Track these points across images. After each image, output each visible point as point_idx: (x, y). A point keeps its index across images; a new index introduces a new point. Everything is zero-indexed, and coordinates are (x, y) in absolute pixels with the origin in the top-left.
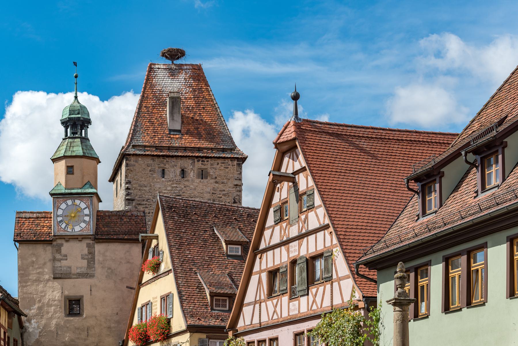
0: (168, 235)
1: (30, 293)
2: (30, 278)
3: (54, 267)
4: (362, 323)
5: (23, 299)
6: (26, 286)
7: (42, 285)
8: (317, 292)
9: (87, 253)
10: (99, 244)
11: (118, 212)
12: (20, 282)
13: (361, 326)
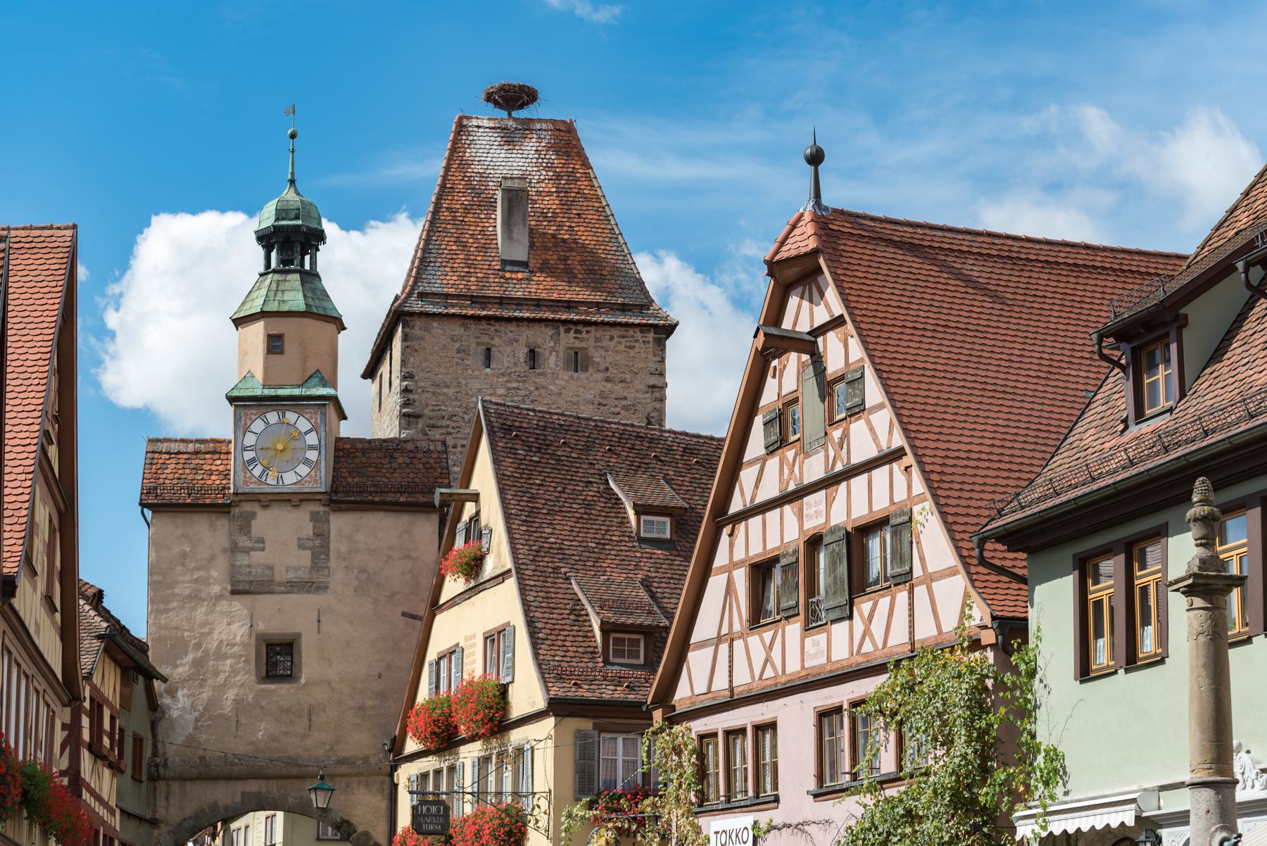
0: (502, 491)
1: (176, 628)
2: (176, 591)
3: (233, 566)
4: (989, 683)
5: (159, 640)
6: (167, 611)
7: (204, 609)
8: (873, 610)
9: (311, 534)
10: (339, 515)
11: (385, 441)
12: (152, 601)
13: (986, 689)
